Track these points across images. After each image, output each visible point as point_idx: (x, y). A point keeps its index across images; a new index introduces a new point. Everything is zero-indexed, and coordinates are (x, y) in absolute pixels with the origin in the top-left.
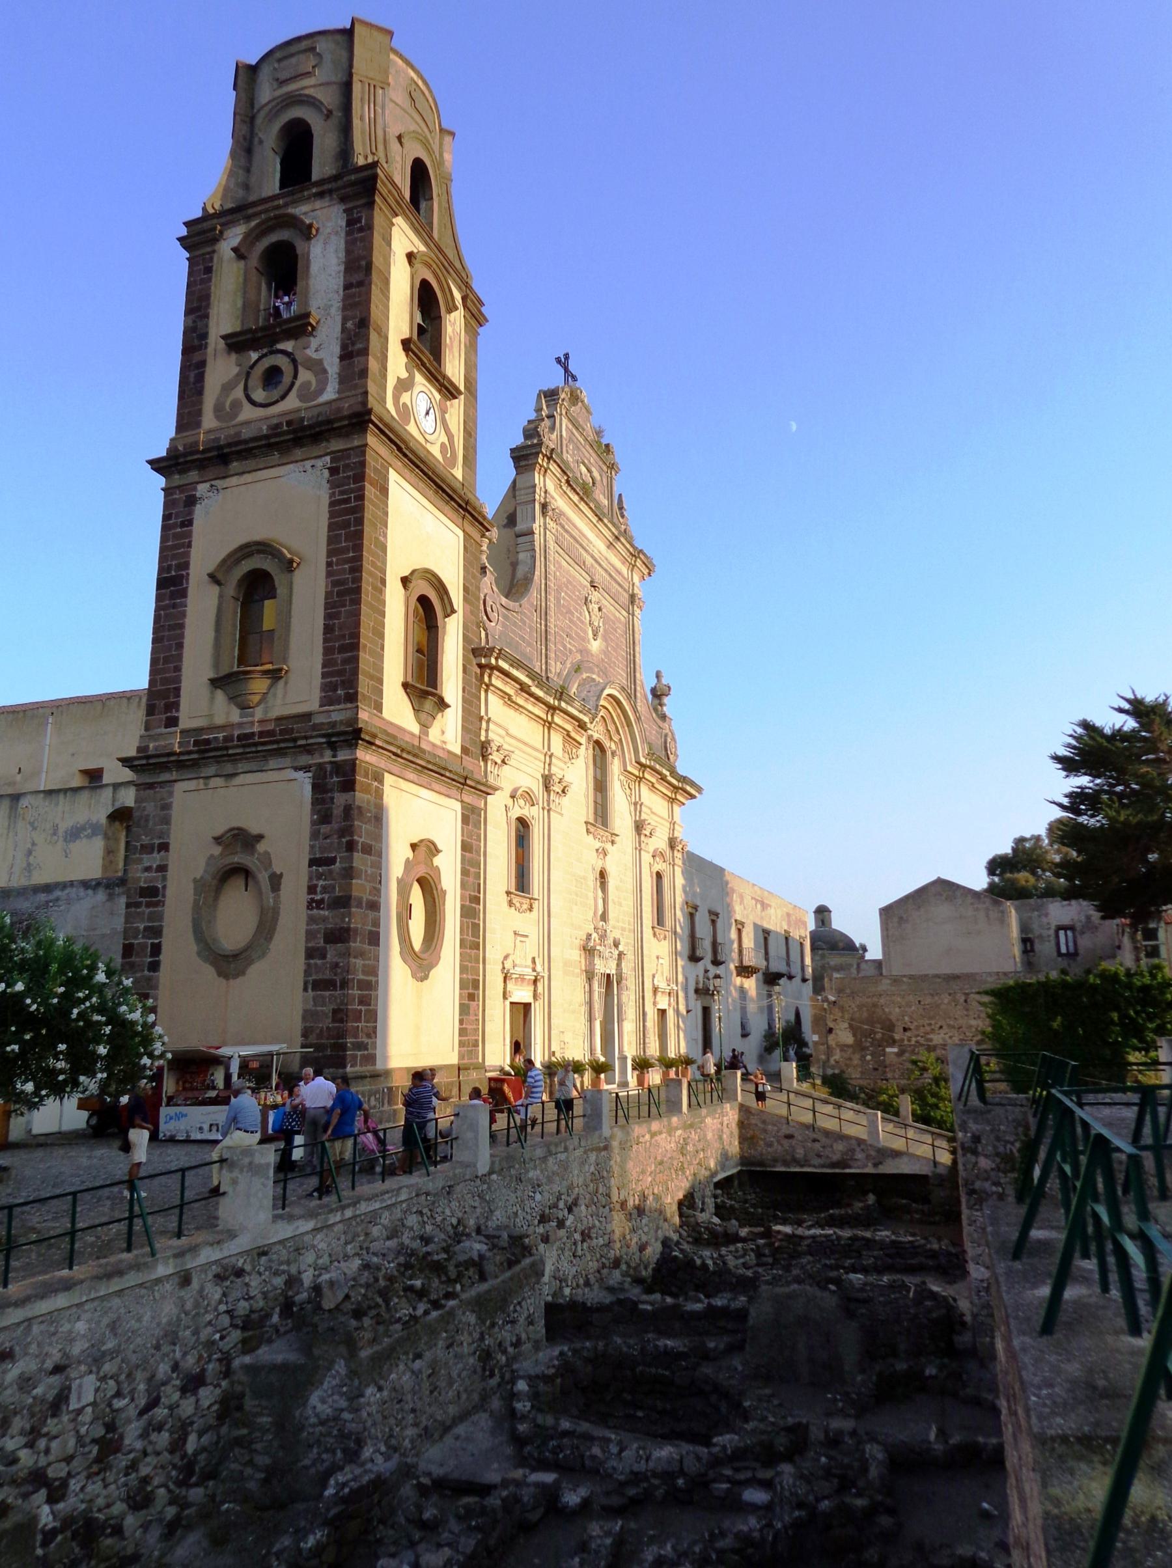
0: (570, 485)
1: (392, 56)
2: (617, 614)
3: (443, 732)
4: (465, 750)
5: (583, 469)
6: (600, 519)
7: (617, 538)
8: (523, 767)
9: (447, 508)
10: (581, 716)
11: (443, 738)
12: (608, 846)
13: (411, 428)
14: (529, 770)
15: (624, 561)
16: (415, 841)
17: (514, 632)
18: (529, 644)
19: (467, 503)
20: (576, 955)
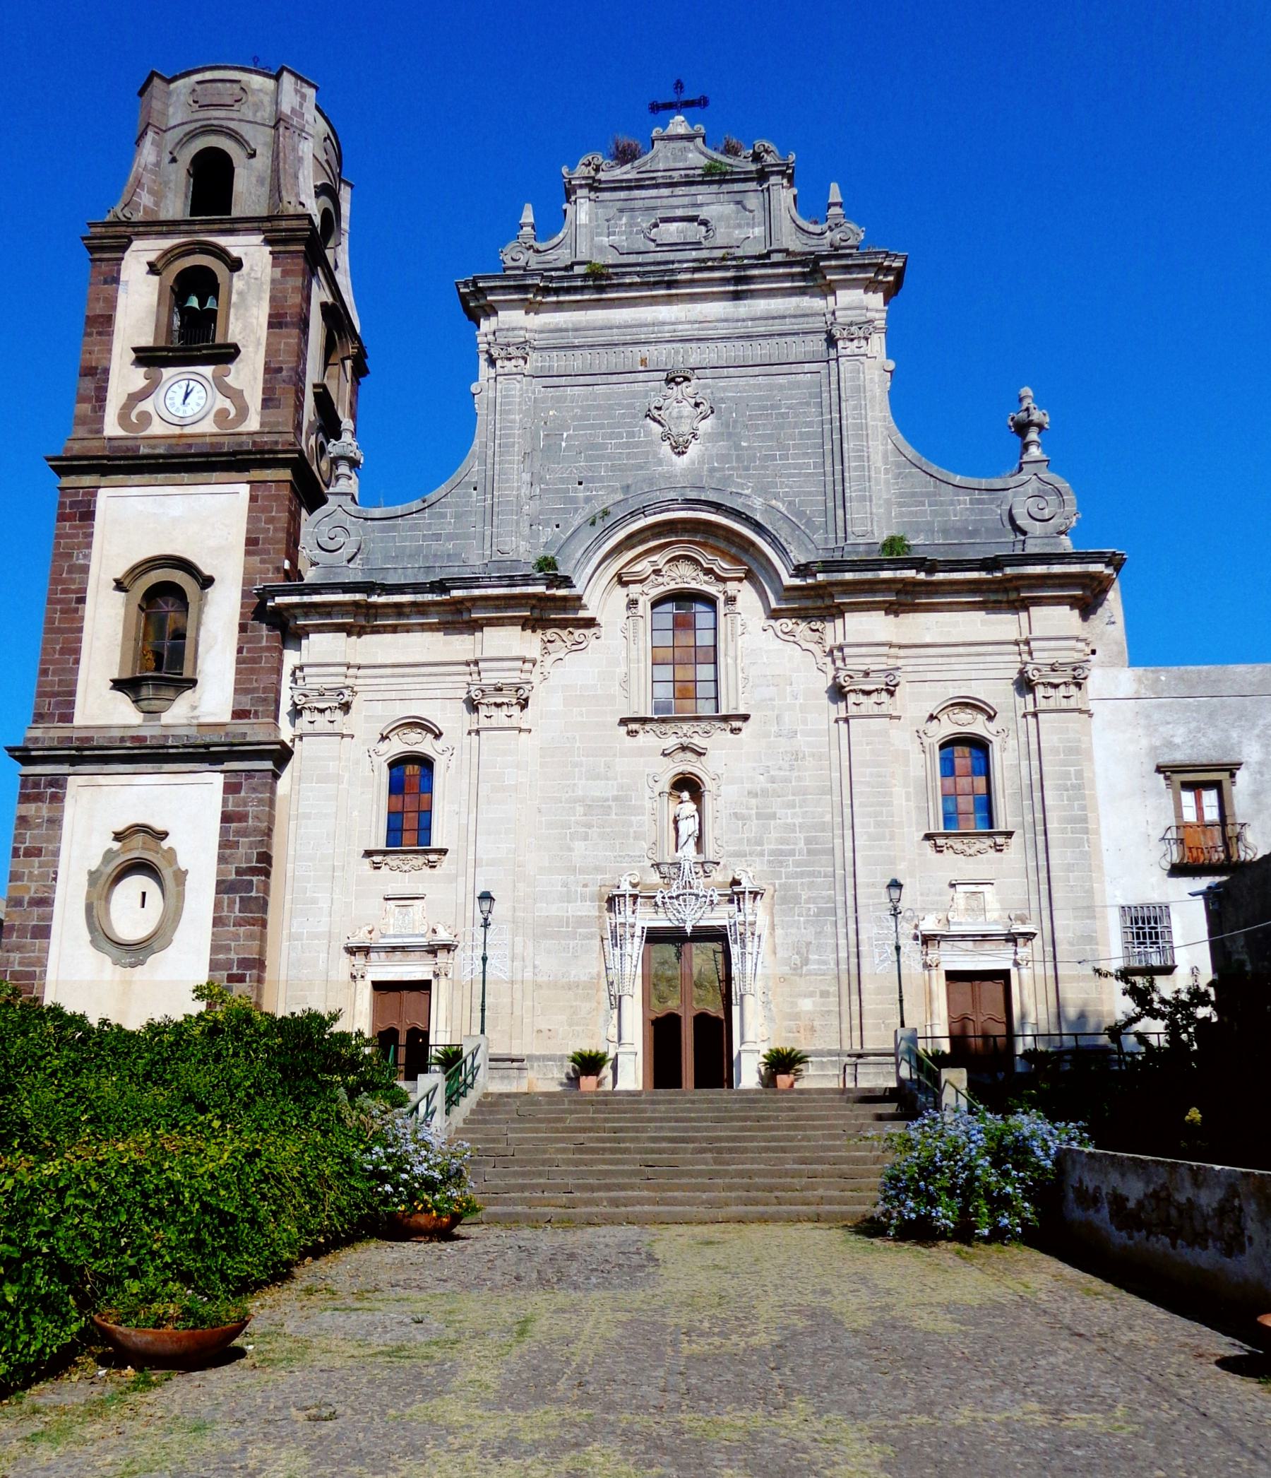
0: (557, 291)
1: (173, 86)
2: (782, 380)
3: (194, 708)
4: (238, 714)
5: (672, 231)
6: (670, 284)
7: (738, 280)
8: (413, 694)
9: (215, 476)
10: (517, 590)
11: (196, 713)
12: (717, 742)
13: (157, 428)
14: (438, 694)
15: (802, 292)
16: (120, 828)
17: (416, 539)
18: (451, 537)
19: (234, 454)
20: (591, 909)
